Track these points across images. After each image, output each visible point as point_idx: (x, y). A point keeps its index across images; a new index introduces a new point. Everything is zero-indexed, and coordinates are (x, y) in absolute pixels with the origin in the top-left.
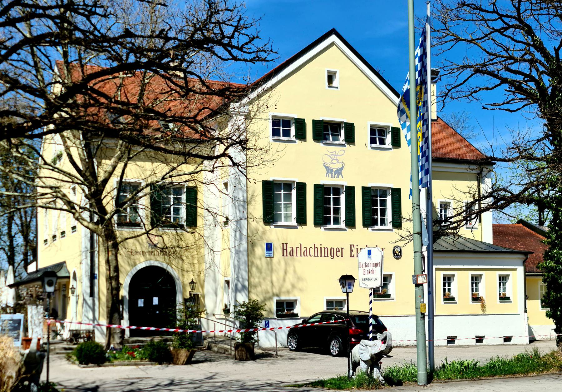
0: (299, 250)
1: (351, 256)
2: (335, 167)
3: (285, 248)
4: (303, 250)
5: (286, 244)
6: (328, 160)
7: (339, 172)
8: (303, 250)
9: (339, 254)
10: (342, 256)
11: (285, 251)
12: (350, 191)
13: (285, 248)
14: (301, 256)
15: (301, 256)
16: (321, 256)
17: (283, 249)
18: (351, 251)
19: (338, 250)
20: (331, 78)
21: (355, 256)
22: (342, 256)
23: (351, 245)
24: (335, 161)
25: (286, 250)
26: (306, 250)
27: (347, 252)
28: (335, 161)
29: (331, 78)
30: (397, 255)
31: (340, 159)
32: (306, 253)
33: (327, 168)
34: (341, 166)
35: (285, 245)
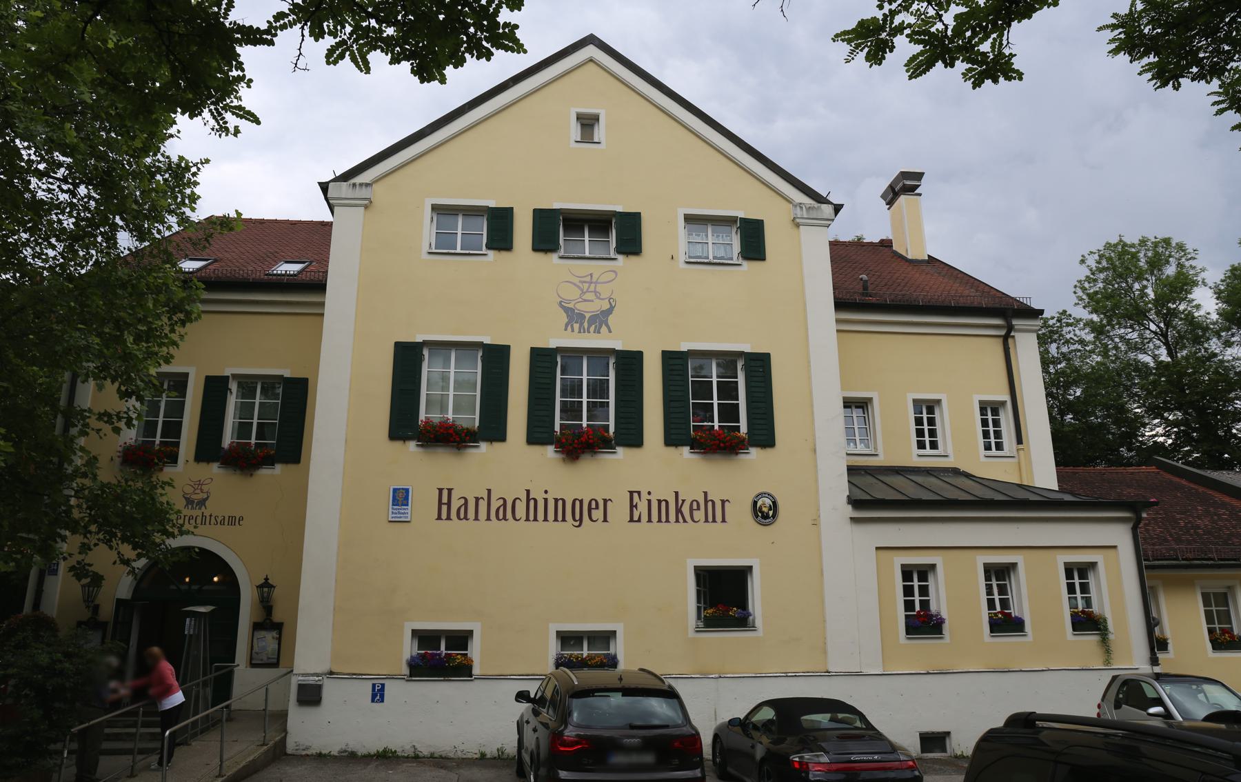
0: (483, 505)
1: (631, 520)
2: (592, 307)
3: (445, 500)
4: (495, 504)
5: (450, 490)
6: (571, 294)
7: (600, 320)
8: (495, 504)
9: (598, 514)
10: (605, 520)
11: (444, 508)
12: (630, 363)
13: (445, 500)
14: (488, 519)
15: (488, 519)
16: (546, 519)
17: (440, 503)
18: (633, 506)
19: (593, 505)
20: (588, 123)
21: (645, 518)
22: (605, 520)
23: (631, 493)
24: (589, 296)
25: (449, 504)
26: (505, 504)
27: (620, 510)
28: (589, 296)
29: (588, 123)
30: (765, 517)
31: (605, 291)
32: (505, 511)
33: (566, 310)
34: (606, 306)
35: (445, 493)
